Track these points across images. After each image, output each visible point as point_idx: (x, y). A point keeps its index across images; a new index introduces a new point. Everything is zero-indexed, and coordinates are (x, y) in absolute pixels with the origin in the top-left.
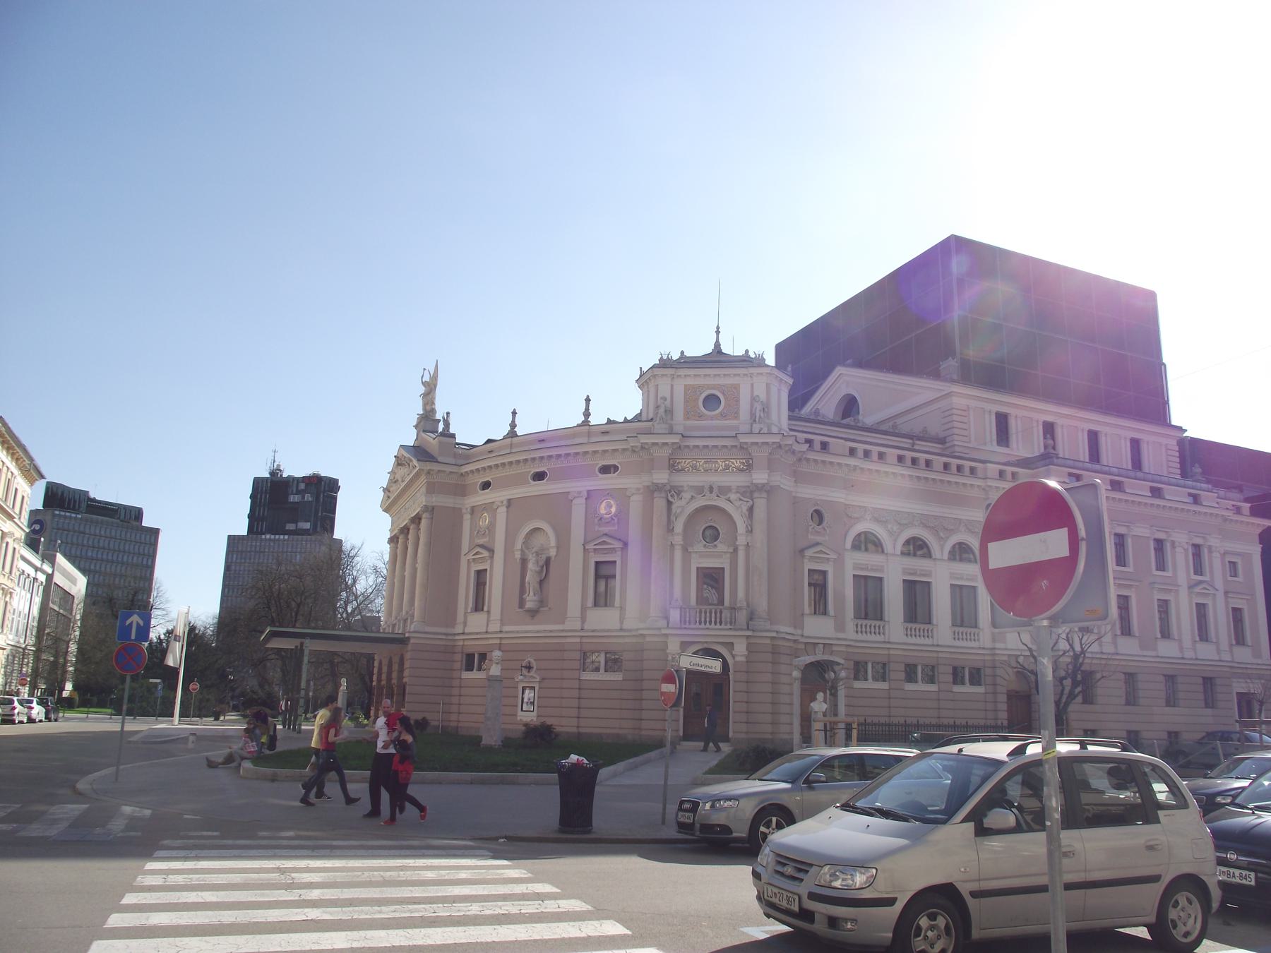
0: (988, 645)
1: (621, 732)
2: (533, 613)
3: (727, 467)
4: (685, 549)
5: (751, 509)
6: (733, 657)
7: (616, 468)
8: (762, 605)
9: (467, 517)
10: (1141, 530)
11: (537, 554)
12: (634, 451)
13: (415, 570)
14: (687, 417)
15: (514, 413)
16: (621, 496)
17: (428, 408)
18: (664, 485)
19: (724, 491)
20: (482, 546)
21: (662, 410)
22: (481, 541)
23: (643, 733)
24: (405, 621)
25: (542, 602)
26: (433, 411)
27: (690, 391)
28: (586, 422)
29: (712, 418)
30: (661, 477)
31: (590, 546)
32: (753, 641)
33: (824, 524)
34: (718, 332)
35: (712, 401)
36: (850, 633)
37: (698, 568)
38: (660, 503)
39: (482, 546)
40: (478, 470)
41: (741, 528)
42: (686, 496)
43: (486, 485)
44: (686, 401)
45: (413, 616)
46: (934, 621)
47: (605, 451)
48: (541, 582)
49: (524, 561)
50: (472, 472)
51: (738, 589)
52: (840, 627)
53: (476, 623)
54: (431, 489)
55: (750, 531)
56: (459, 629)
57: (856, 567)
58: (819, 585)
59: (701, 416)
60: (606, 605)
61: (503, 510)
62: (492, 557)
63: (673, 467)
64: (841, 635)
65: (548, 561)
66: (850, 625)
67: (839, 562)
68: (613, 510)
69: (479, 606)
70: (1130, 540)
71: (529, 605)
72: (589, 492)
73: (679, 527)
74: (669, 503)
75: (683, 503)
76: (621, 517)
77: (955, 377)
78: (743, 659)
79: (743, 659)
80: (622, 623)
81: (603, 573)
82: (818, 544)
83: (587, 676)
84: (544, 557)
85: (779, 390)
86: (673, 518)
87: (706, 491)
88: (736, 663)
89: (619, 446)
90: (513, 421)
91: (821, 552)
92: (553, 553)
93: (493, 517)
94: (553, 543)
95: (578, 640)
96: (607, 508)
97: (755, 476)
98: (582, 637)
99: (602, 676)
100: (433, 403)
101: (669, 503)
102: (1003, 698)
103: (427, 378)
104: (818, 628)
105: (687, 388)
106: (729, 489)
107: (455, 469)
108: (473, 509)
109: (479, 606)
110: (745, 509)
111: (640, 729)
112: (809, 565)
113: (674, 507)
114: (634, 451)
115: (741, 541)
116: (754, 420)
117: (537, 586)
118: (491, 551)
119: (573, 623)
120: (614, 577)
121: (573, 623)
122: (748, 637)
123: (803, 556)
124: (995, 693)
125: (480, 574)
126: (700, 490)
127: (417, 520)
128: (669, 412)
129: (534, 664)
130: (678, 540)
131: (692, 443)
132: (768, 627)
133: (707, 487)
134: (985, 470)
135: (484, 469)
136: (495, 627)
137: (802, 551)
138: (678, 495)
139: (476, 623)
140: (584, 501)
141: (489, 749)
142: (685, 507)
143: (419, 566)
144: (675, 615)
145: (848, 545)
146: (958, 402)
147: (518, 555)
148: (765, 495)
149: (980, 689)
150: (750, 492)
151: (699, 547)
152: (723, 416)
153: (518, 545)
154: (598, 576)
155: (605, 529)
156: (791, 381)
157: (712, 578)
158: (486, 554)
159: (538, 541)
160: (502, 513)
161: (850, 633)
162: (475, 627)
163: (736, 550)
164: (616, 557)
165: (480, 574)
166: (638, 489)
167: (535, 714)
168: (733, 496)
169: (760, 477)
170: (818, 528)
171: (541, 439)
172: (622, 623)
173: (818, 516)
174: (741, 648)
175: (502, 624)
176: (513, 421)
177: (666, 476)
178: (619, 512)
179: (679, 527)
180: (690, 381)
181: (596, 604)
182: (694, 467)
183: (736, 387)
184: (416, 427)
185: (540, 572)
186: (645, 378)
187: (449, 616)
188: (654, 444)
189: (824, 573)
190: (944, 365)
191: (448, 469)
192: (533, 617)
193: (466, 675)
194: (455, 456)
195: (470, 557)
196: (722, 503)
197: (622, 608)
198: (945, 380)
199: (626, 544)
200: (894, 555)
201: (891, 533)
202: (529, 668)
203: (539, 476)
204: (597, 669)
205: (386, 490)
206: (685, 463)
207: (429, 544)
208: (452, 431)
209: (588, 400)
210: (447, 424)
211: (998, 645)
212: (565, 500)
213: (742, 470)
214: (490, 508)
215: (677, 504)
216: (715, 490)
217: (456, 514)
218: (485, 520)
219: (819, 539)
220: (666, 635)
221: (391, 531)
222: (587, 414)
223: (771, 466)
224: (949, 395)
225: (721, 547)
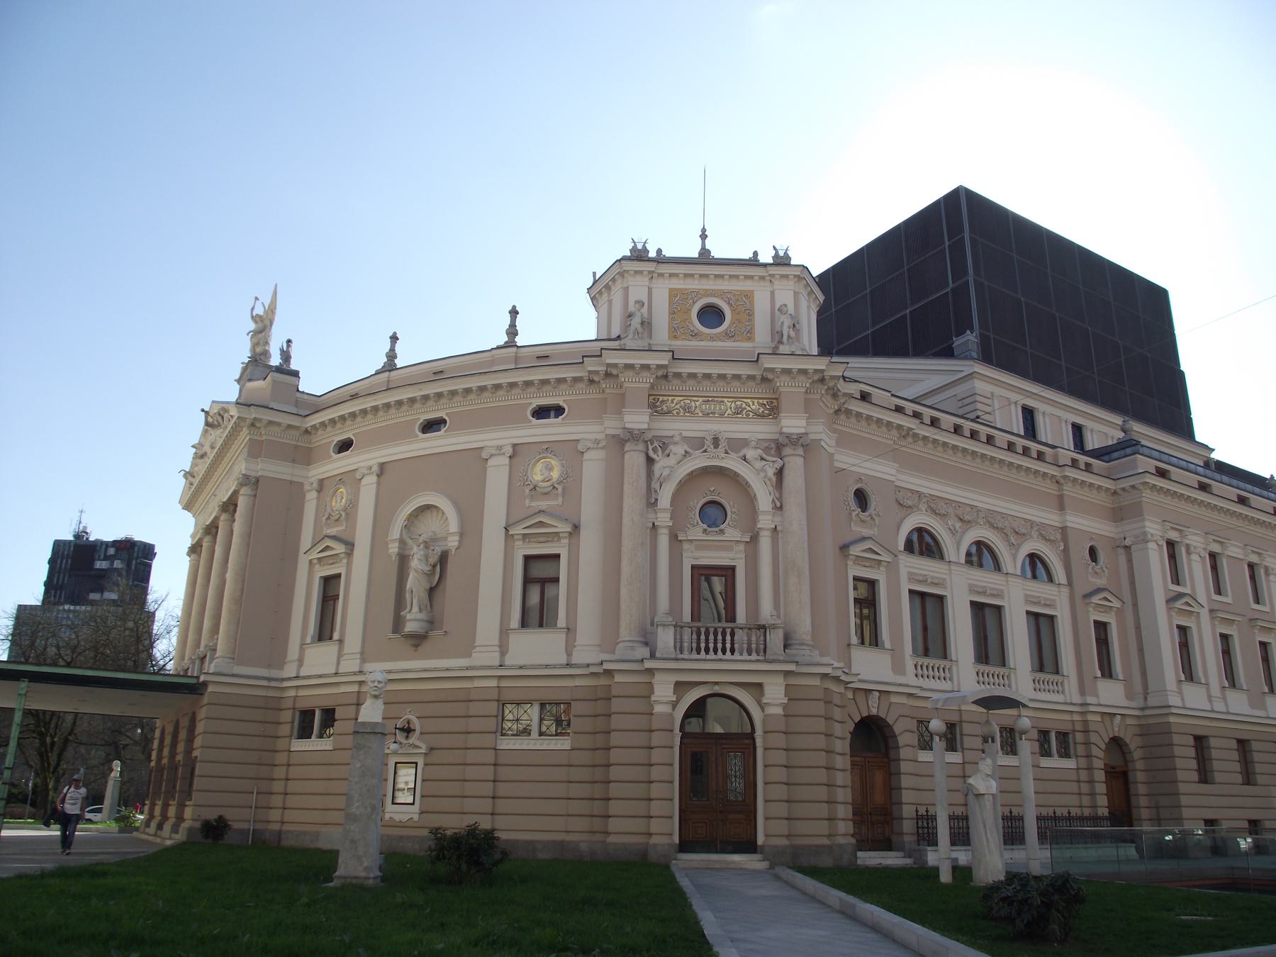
0: (1077, 699)
1: (568, 838)
2: (418, 639)
3: (738, 411)
4: (674, 538)
5: (780, 473)
6: (762, 707)
7: (559, 410)
8: (804, 626)
9: (311, 496)
10: (1234, 550)
11: (427, 545)
12: (592, 381)
13: (223, 582)
14: (674, 333)
15: (394, 338)
16: (572, 452)
17: (258, 350)
18: (643, 432)
19: (736, 445)
20: (334, 538)
21: (636, 322)
22: (333, 531)
23: (611, 839)
24: (203, 659)
25: (432, 623)
26: (266, 354)
27: (678, 300)
28: (511, 344)
29: (712, 338)
30: (637, 419)
31: (517, 530)
32: (793, 681)
33: (871, 510)
34: (704, 236)
35: (711, 315)
36: (910, 678)
37: (693, 567)
38: (634, 459)
39: (334, 538)
40: (333, 421)
41: (764, 501)
42: (678, 450)
43: (345, 446)
44: (672, 313)
45: (215, 650)
46: (1011, 662)
47: (545, 382)
48: (432, 591)
49: (403, 559)
50: (323, 424)
51: (762, 599)
52: (898, 668)
53: (320, 660)
54: (256, 450)
55: (779, 508)
56: (290, 671)
57: (912, 578)
58: (868, 603)
59: (695, 335)
60: (541, 625)
61: (371, 480)
62: (349, 554)
63: (655, 407)
64: (901, 679)
65: (443, 558)
66: (909, 663)
67: (892, 568)
68: (555, 475)
69: (324, 632)
70: (1224, 561)
71: (410, 627)
72: (514, 446)
73: (665, 498)
74: (650, 461)
75: (672, 461)
76: (569, 485)
77: (975, 355)
78: (779, 711)
79: (779, 711)
80: (569, 654)
81: (539, 575)
82: (864, 539)
83: (506, 744)
84: (438, 550)
85: (809, 307)
86: (655, 485)
87: (708, 443)
88: (766, 718)
89: (569, 373)
90: (392, 349)
91: (871, 550)
92: (453, 543)
93: (356, 494)
94: (454, 526)
95: (494, 683)
96: (543, 471)
97: (785, 422)
98: (500, 677)
99: (533, 743)
100: (267, 343)
101: (650, 461)
102: (1100, 775)
103: (259, 311)
104: (871, 667)
105: (673, 293)
106: (745, 443)
107: (295, 421)
108: (321, 482)
109: (324, 632)
110: (771, 472)
111: (607, 833)
112: (854, 571)
113: (657, 468)
114: (592, 381)
115: (765, 522)
116: (778, 337)
117: (425, 596)
118: (350, 545)
119: (485, 655)
120: (556, 580)
121: (485, 655)
122: (787, 674)
123: (846, 556)
124: (1090, 769)
125: (330, 582)
126: (698, 443)
127: (230, 506)
128: (647, 324)
129: (416, 724)
130: (664, 519)
131: (686, 368)
132: (819, 659)
133: (709, 438)
134: (1056, 456)
135: (343, 418)
136: (350, 665)
137: (844, 548)
138: (664, 446)
139: (320, 660)
140: (507, 461)
141: (355, 889)
142: (675, 468)
143: (229, 576)
144: (665, 639)
145: (901, 545)
146: (980, 386)
147: (394, 549)
148: (800, 451)
149: (1070, 763)
150: (778, 447)
151: (697, 532)
152: (728, 335)
153: (395, 533)
154: (527, 581)
155: (543, 504)
156: (821, 298)
157: (713, 582)
158: (340, 548)
159: (429, 526)
160: (369, 487)
161: (910, 678)
162: (315, 666)
163: (755, 539)
164: (561, 548)
165: (330, 582)
166: (597, 442)
167: (416, 808)
168: (751, 453)
169: (793, 423)
170: (864, 516)
171: (438, 371)
172: (569, 654)
173: (861, 498)
174: (775, 692)
175: (364, 660)
176: (392, 349)
177: (646, 418)
178: (564, 478)
179: (665, 498)
180: (677, 284)
181: (524, 624)
182: (687, 409)
183: (749, 295)
184: (238, 381)
185: (430, 575)
186: (599, 287)
187: (275, 652)
188: (629, 367)
189: (872, 584)
190: (958, 342)
191: (286, 420)
192: (416, 646)
193: (299, 745)
194: (297, 403)
195: (314, 555)
196: (732, 463)
197: (570, 630)
198: (966, 358)
199: (576, 527)
200: (957, 563)
201: (953, 532)
202: (408, 731)
203: (431, 426)
204: (526, 732)
205: (189, 475)
206: (673, 403)
207: (248, 535)
208: (293, 366)
209: (514, 313)
210: (286, 356)
211: (1090, 700)
212: (477, 459)
213: (762, 416)
214: (351, 479)
215: (662, 464)
216: (723, 444)
217: (295, 491)
218: (338, 503)
219: (866, 532)
220: (651, 671)
221: (193, 536)
222: (512, 331)
223: (809, 408)
224: (970, 376)
225: (732, 533)
